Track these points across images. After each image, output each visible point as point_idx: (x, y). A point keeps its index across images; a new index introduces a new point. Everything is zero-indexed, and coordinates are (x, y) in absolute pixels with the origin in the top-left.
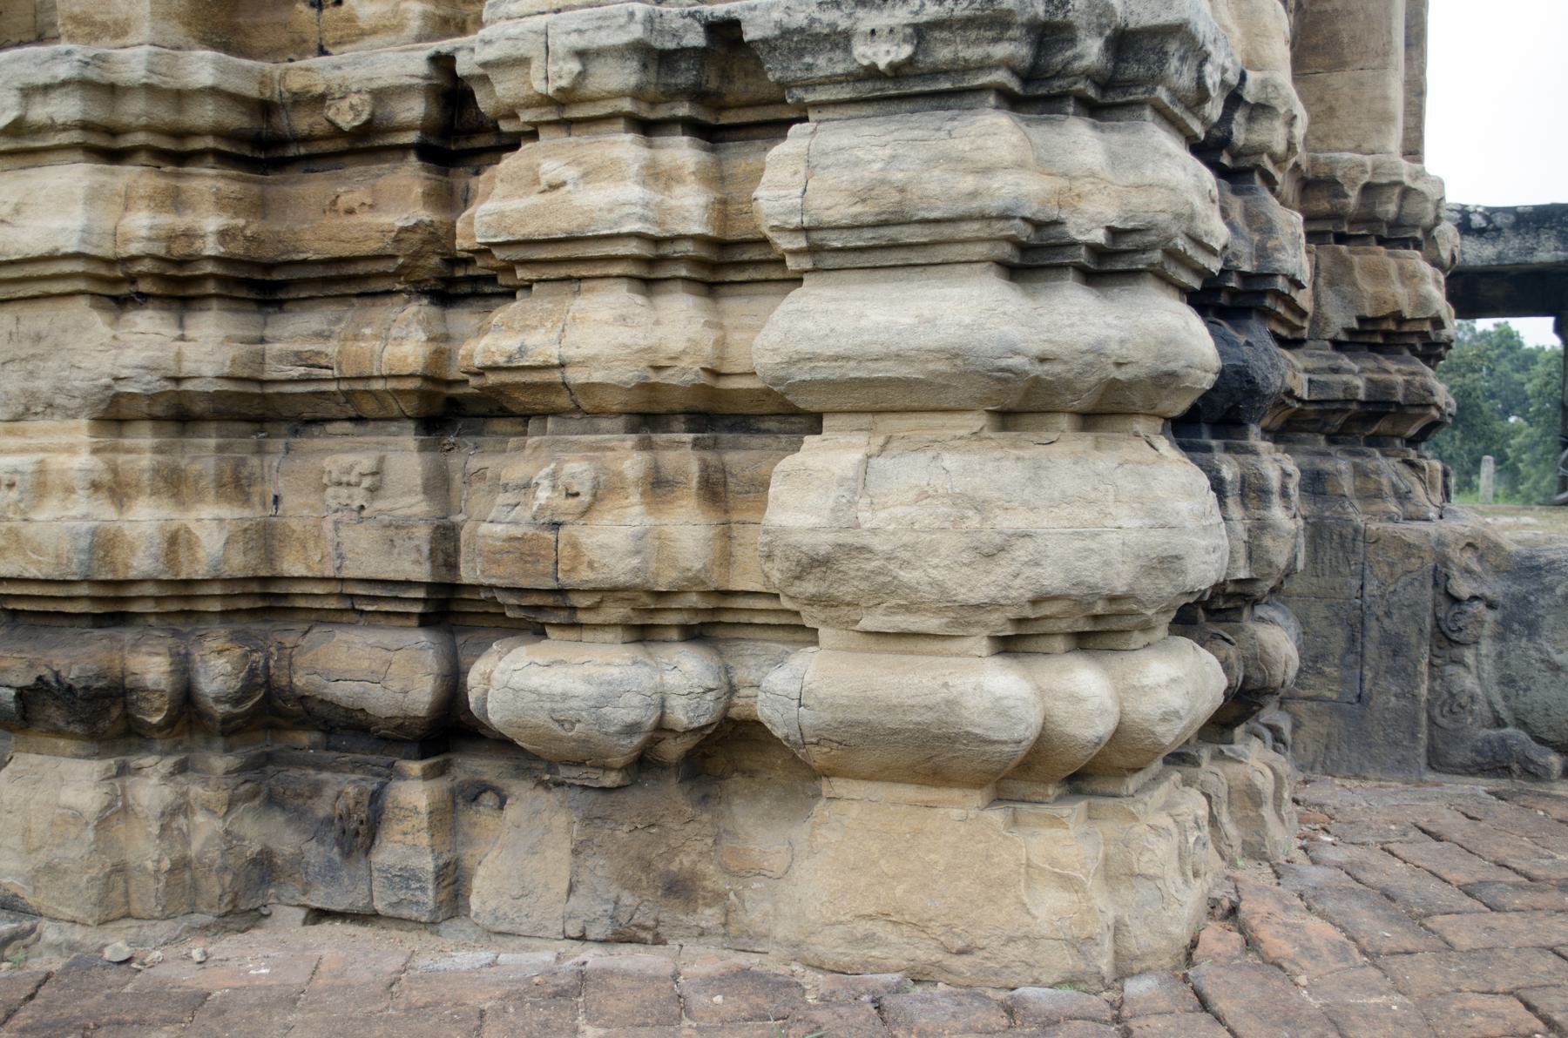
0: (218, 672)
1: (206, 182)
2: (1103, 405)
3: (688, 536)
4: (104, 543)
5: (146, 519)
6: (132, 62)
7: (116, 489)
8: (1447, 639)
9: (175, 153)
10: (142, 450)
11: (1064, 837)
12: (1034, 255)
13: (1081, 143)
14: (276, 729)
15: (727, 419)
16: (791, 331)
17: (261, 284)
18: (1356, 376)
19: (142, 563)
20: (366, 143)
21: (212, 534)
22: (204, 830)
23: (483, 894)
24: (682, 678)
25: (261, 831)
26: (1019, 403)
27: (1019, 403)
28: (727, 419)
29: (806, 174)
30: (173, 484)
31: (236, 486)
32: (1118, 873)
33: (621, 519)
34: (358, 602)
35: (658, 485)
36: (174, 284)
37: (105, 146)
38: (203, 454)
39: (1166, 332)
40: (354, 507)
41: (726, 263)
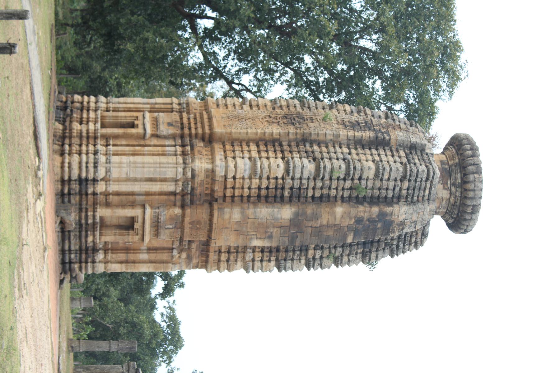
0: (67, 134)
1: (93, 135)
2: (80, 168)
3: (74, 151)
4: (74, 129)
5: (75, 131)
6: (99, 131)
7: (77, 130)
8: (65, 210)
9: (95, 133)
10: (79, 132)
11: (59, 165)
12: (87, 163)
13: (92, 165)
14: (63, 137)
15: (80, 154)
16: (84, 157)
17: (88, 137)
18: (84, 206)
19: (73, 131)
20: (95, 142)
21: (75, 134)
22: (58, 134)
23: (55, 145)
24: (67, 152)
25: (58, 136)
26: (80, 163)
27: (80, 163)
28: (80, 154)
29: (91, 156)
30: (77, 133)
31: (77, 136)
32: (57, 167)
33: (75, 148)
34: (70, 141)
35: (76, 150)
36: (88, 132)
37: (95, 130)
38: (79, 134)
39: (84, 175)
40: (76, 141)
41: (87, 154)
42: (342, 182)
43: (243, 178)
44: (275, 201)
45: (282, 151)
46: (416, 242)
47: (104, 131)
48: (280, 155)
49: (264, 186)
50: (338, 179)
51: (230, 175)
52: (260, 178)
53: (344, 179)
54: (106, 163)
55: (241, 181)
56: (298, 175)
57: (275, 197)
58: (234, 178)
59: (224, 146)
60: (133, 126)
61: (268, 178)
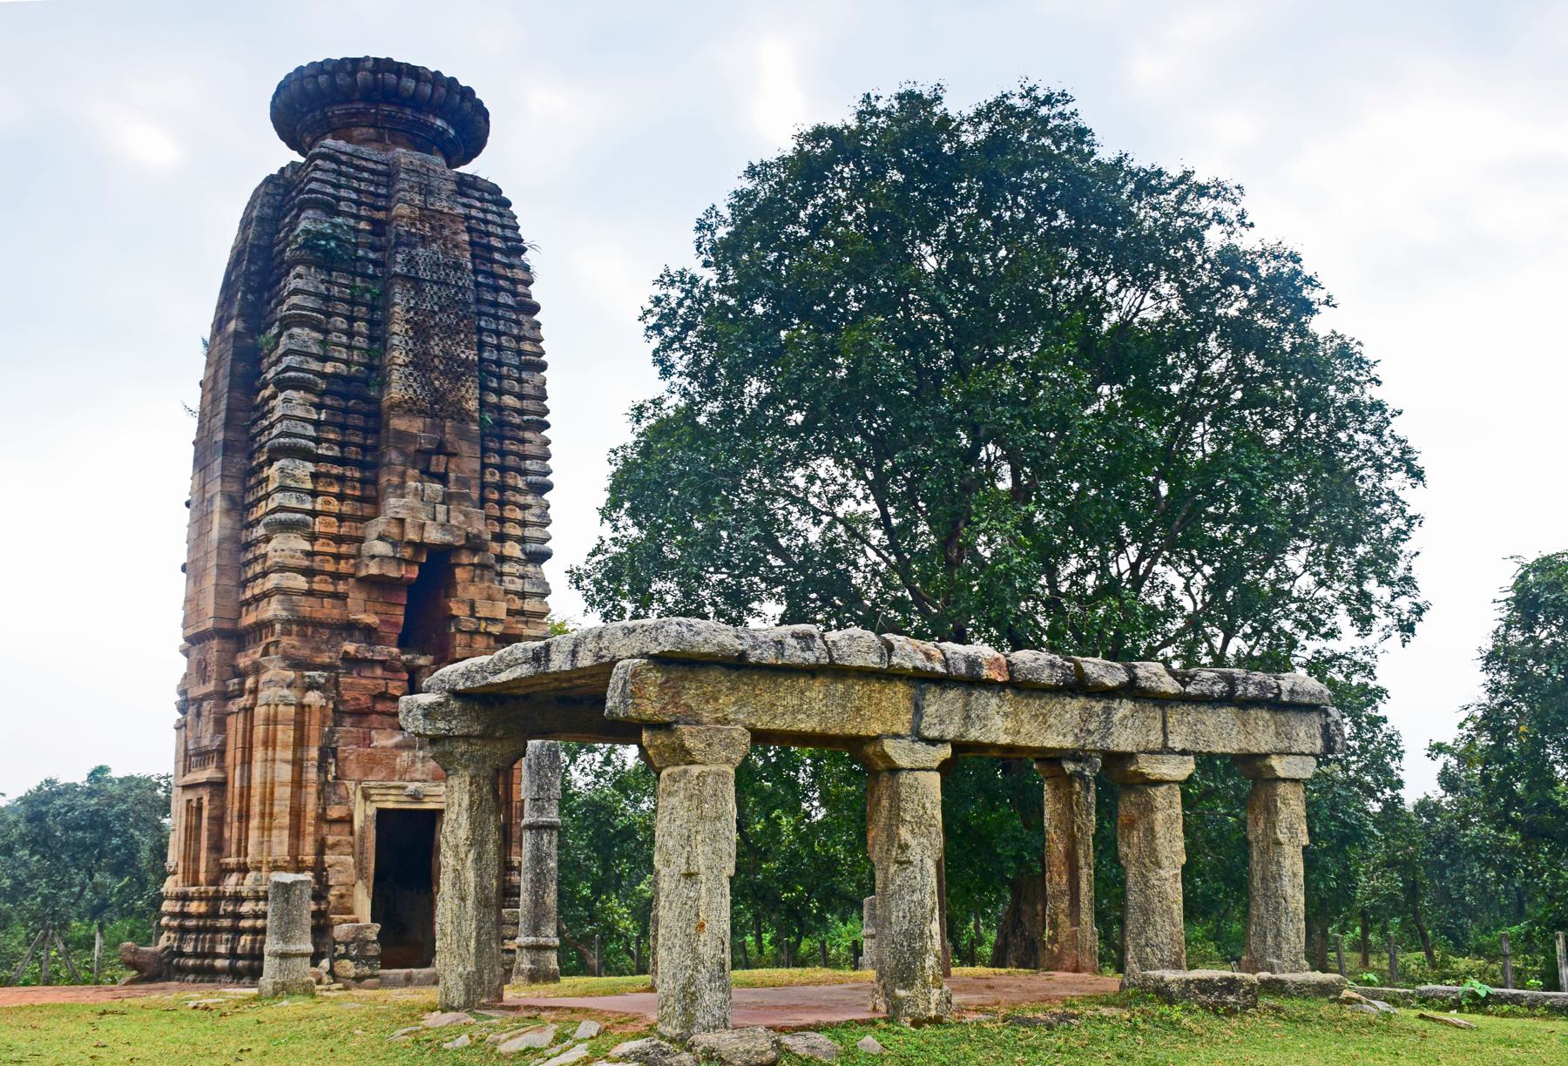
42: (333, 337)
43: (310, 555)
44: (375, 482)
45: (261, 467)
46: (495, 203)
47: (202, 877)
48: (266, 472)
49: (335, 506)
50: (323, 343)
51: (300, 582)
52: (314, 514)
53: (326, 332)
54: (259, 869)
55: (318, 558)
56: (310, 431)
57: (363, 481)
58: (309, 573)
59: (247, 603)
60: (200, 809)
61: (314, 494)
